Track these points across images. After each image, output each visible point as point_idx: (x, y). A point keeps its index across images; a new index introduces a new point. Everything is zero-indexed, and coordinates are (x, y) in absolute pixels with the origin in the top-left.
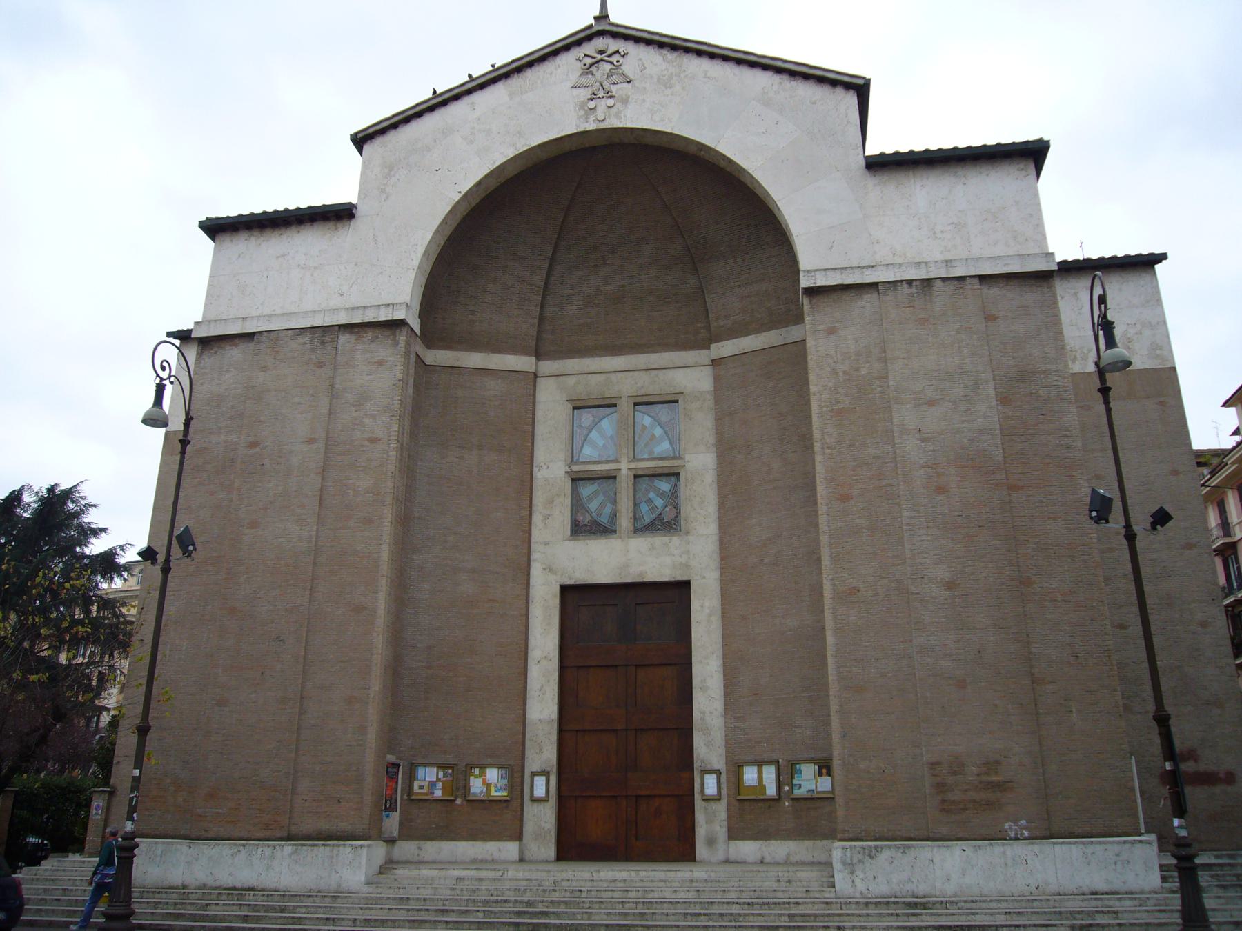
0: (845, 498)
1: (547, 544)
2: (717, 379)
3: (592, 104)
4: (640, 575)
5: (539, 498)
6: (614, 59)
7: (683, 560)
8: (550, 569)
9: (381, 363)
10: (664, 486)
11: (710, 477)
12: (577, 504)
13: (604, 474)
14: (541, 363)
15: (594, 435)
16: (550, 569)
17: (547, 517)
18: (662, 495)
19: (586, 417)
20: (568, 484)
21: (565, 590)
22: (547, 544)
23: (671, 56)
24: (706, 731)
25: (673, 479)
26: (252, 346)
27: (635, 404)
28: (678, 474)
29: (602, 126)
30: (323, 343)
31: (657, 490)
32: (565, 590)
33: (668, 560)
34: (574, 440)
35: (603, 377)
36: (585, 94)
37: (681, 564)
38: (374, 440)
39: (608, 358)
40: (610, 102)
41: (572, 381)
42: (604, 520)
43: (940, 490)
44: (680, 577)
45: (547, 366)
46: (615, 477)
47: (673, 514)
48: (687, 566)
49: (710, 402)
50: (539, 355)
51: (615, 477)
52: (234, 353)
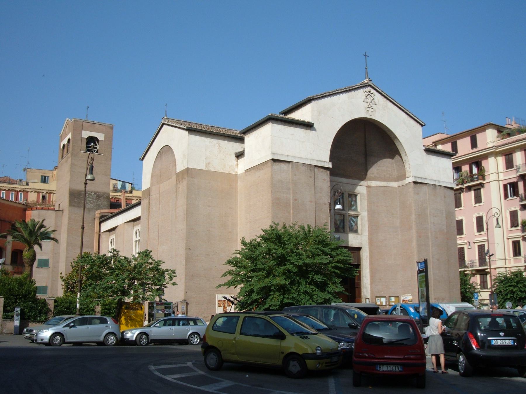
0: (420, 237)
3: (368, 109)
6: (372, 95)
9: (324, 180)
11: (366, 219)
18: (354, 222)
23: (385, 99)
24: (366, 288)
26: (290, 166)
29: (370, 117)
30: (311, 170)
33: (358, 241)
36: (366, 105)
38: (325, 204)
40: (372, 110)
43: (437, 238)
49: (366, 198)
52: (283, 166)
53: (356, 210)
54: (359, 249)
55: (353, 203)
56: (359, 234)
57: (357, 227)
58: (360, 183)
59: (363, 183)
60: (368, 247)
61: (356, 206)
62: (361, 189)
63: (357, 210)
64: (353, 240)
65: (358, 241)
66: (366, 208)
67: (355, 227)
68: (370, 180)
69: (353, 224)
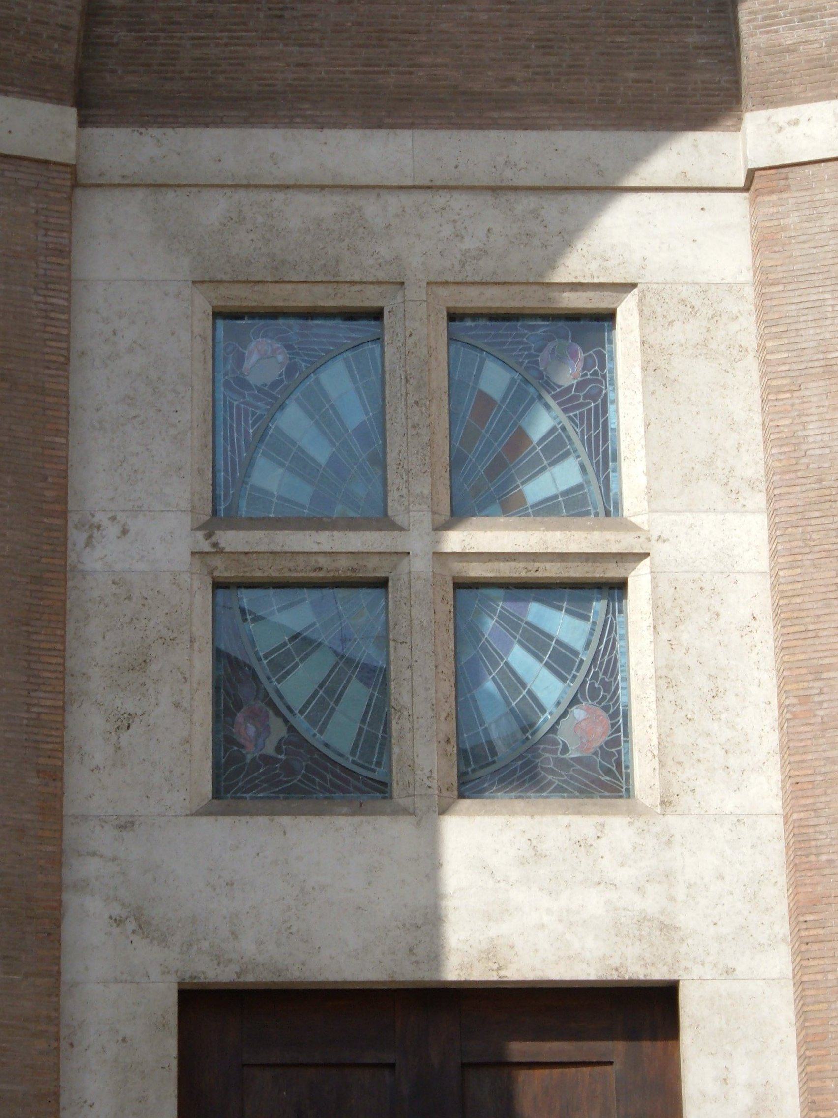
1: (126, 825)
2: (765, 241)
4: (490, 954)
5: (96, 644)
7: (651, 903)
8: (138, 921)
10: (562, 625)
11: (750, 595)
12: (235, 684)
13: (342, 567)
14: (98, 134)
15: (293, 421)
16: (138, 921)
17: (125, 722)
18: (561, 661)
19: (264, 356)
20: (201, 601)
21: (198, 1003)
22: (126, 825)
25: (599, 606)
27: (453, 317)
28: (617, 588)
31: (537, 641)
32: (198, 1003)
33: (594, 903)
34: (236, 430)
35: (326, 207)
37: (643, 919)
39: (351, 136)
41: (213, 210)
42: (340, 735)
44: (637, 965)
45: (122, 148)
46: (382, 584)
47: (600, 734)
48: (667, 928)
49: (745, 328)
50: (91, 105)
51: (382, 584)
53: (596, 500)
54: (645, 1011)
55: (542, 423)
56: (634, 812)
57: (619, 721)
58: (638, 158)
59: (684, 154)
60: (779, 962)
61: (603, 456)
62: (666, 235)
63: (611, 507)
64: (510, 896)
65: (594, 903)
66: (751, 462)
67: (581, 732)
68: (779, 95)
69: (548, 688)
